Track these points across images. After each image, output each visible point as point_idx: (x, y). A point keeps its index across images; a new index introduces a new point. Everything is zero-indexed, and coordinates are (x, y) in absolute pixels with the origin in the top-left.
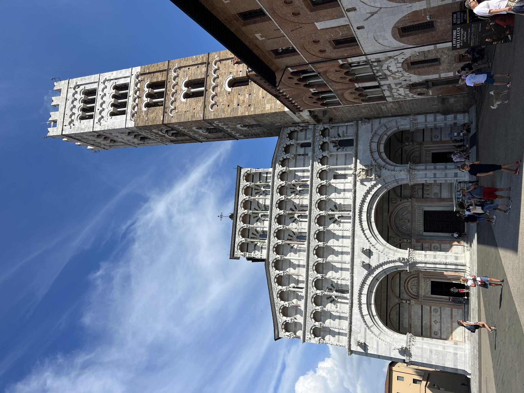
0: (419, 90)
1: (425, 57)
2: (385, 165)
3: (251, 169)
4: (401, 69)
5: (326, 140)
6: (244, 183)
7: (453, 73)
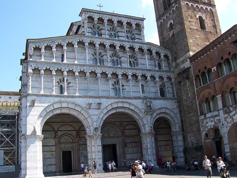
2: (153, 118)
5: (165, 80)
7: (229, 151)
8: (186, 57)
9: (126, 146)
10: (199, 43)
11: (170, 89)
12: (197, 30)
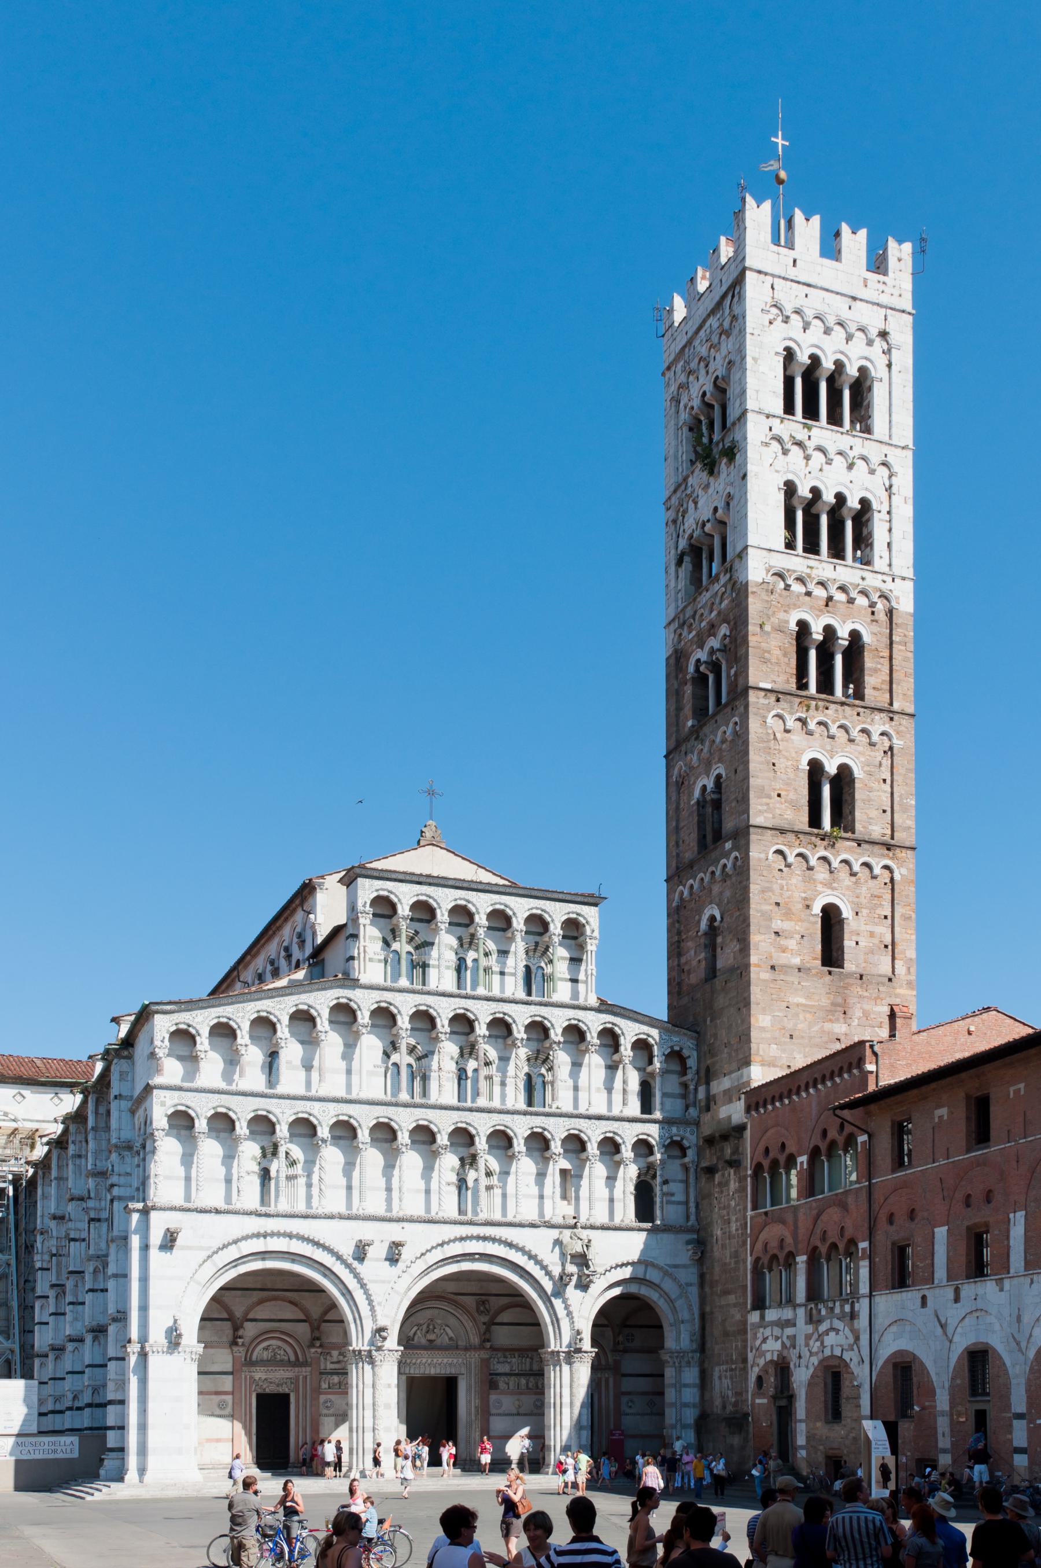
0: (772, 1379)
1: (848, 1398)
3: (595, 938)
4: (827, 1352)
6: (557, 913)
8: (738, 1080)
9: (493, 1385)
10: (800, 1026)
12: (799, 970)
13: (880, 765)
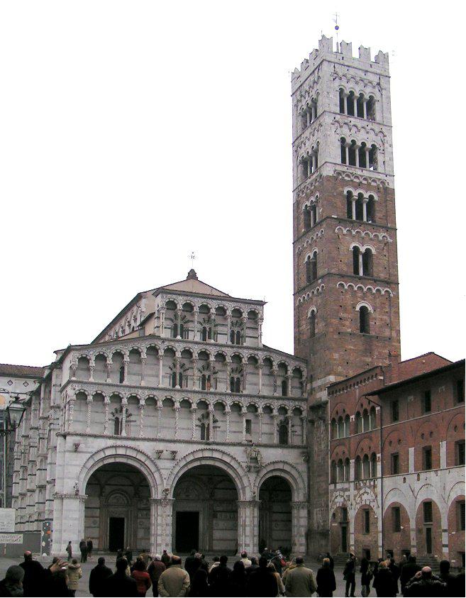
4: (364, 503)
5: (290, 413)
11: (298, 429)
13: (383, 249)
